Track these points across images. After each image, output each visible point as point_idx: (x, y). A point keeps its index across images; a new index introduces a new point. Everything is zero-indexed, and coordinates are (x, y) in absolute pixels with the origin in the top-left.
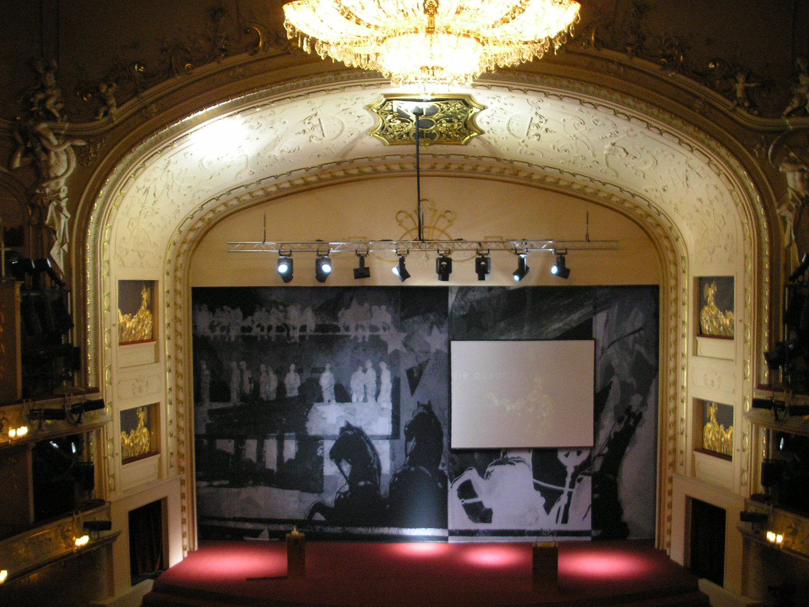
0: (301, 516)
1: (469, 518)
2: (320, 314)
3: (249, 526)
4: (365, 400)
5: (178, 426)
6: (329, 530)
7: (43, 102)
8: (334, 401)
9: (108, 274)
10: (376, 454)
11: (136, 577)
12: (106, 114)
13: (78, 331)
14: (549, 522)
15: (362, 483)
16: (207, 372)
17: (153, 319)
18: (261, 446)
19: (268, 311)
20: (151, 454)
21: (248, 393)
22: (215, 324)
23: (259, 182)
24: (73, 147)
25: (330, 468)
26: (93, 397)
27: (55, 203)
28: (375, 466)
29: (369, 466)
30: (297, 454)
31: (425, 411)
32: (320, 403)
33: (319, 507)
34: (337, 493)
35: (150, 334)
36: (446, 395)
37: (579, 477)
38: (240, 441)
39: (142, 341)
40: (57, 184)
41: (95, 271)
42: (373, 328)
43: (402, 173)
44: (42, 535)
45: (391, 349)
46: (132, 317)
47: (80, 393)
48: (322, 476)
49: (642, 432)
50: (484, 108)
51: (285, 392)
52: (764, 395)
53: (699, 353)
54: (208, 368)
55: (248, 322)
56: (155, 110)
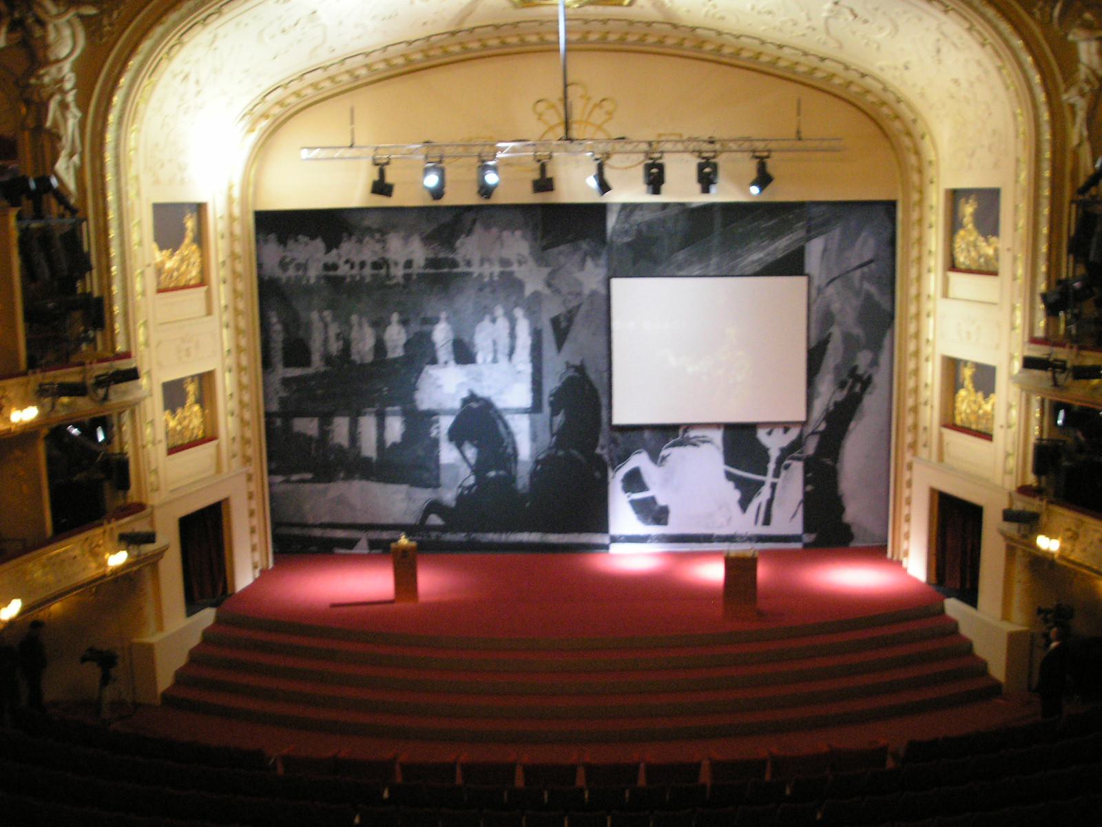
0: (410, 520)
1: (639, 519)
3: (340, 534)
4: (495, 361)
6: (449, 537)
8: (452, 363)
9: (138, 194)
10: (510, 434)
11: (193, 604)
13: (100, 272)
14: (745, 523)
15: (492, 474)
16: (278, 327)
18: (354, 426)
24: (82, 17)
25: (448, 454)
26: (124, 365)
27: (57, 97)
28: (510, 450)
29: (501, 450)
32: (434, 366)
33: (435, 507)
34: (460, 487)
36: (605, 352)
38: (326, 419)
40: (60, 70)
42: (505, 262)
45: (528, 290)
46: (172, 255)
47: (106, 360)
49: (871, 402)
52: (1038, 352)
53: (951, 293)
54: (279, 321)
55: (332, 257)
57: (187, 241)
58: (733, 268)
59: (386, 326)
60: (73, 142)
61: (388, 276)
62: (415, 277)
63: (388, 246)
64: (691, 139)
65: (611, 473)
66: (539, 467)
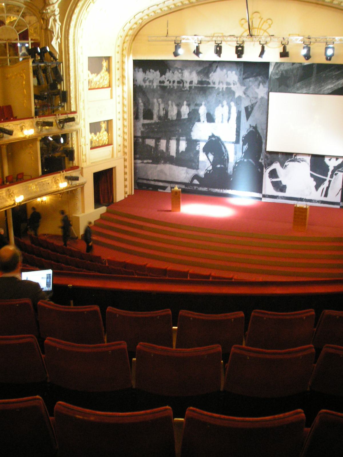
0: (187, 181)
2: (200, 75)
3: (161, 184)
4: (222, 122)
5: (124, 132)
8: (206, 122)
10: (226, 151)
11: (98, 203)
14: (317, 195)
16: (142, 104)
17: (110, 76)
19: (173, 73)
20: (108, 145)
21: (162, 115)
22: (146, 79)
25: (202, 157)
26: (71, 116)
27: (53, 17)
28: (226, 157)
29: (223, 157)
30: (186, 148)
31: (253, 130)
33: (196, 177)
34: (206, 170)
35: (108, 84)
36: (266, 122)
37: (336, 172)
38: (158, 140)
39: (103, 88)
40: (54, 7)
41: (74, 52)
42: (228, 84)
44: (45, 181)
45: (237, 95)
47: (66, 114)
48: (198, 161)
51: (181, 116)
58: (320, 90)
59: (181, 106)
62: (193, 88)
63: (183, 75)
65: (264, 170)
66: (237, 165)
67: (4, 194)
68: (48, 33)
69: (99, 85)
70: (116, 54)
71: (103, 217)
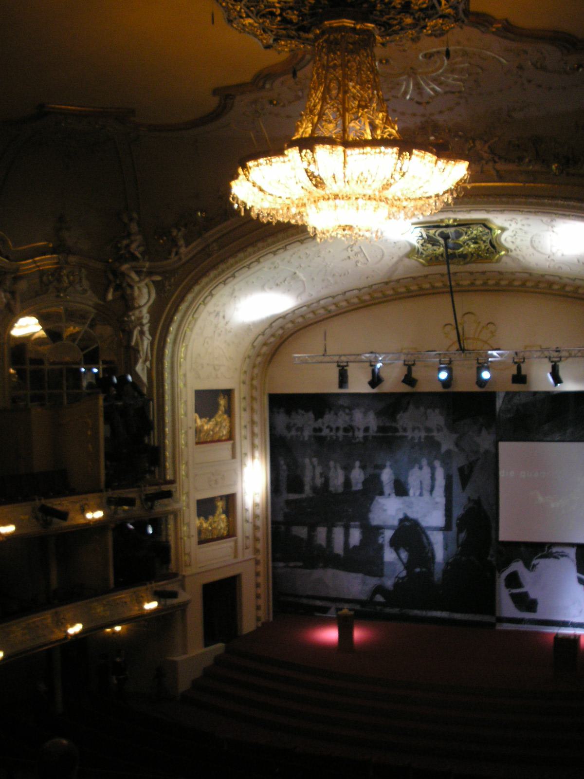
0: (364, 597)
1: (516, 606)
3: (318, 603)
4: (421, 495)
6: (388, 610)
7: (128, 246)
8: (393, 495)
9: (185, 385)
10: (430, 544)
11: (209, 638)
12: (177, 253)
16: (284, 467)
19: (336, 414)
23: (318, 301)
24: (153, 282)
25: (389, 555)
26: (165, 488)
27: (139, 328)
28: (430, 555)
30: (361, 541)
32: (381, 497)
33: (379, 589)
34: (397, 577)
38: (312, 528)
39: (219, 441)
40: (141, 312)
42: (428, 430)
43: (432, 292)
44: (121, 598)
45: (444, 448)
46: (209, 421)
47: (156, 485)
50: (503, 229)
56: (216, 248)
57: (220, 412)
60: (147, 354)
61: (354, 437)
64: (547, 349)
65: (497, 574)
66: (449, 567)
67: (49, 621)
68: (131, 354)
69: (213, 436)
70: (242, 385)
71: (218, 661)
